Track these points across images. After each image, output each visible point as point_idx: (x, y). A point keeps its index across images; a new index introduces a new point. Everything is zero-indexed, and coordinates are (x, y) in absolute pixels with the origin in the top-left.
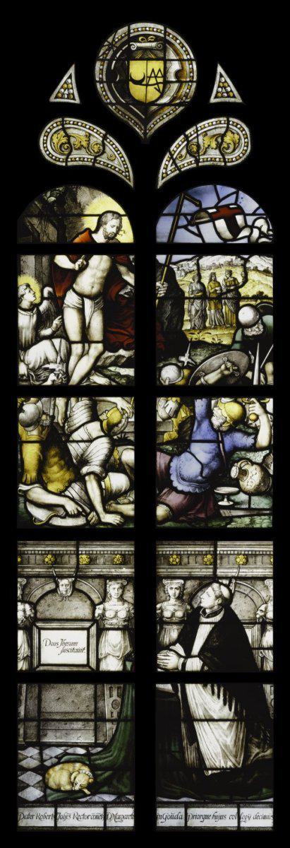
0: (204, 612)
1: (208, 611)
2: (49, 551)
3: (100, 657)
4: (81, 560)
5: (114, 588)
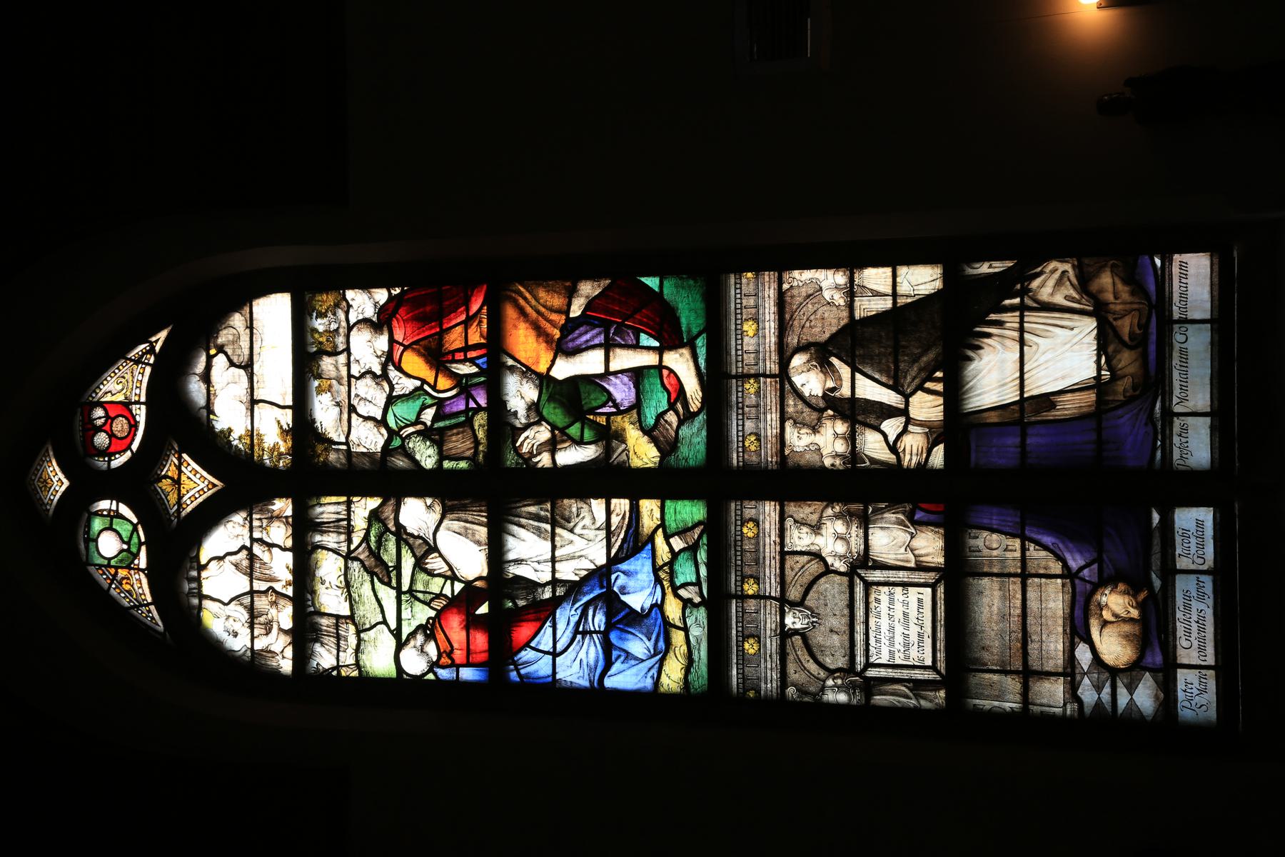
0: (833, 390)
1: (830, 384)
2: (737, 646)
3: (912, 565)
4: (751, 592)
5: (800, 539)
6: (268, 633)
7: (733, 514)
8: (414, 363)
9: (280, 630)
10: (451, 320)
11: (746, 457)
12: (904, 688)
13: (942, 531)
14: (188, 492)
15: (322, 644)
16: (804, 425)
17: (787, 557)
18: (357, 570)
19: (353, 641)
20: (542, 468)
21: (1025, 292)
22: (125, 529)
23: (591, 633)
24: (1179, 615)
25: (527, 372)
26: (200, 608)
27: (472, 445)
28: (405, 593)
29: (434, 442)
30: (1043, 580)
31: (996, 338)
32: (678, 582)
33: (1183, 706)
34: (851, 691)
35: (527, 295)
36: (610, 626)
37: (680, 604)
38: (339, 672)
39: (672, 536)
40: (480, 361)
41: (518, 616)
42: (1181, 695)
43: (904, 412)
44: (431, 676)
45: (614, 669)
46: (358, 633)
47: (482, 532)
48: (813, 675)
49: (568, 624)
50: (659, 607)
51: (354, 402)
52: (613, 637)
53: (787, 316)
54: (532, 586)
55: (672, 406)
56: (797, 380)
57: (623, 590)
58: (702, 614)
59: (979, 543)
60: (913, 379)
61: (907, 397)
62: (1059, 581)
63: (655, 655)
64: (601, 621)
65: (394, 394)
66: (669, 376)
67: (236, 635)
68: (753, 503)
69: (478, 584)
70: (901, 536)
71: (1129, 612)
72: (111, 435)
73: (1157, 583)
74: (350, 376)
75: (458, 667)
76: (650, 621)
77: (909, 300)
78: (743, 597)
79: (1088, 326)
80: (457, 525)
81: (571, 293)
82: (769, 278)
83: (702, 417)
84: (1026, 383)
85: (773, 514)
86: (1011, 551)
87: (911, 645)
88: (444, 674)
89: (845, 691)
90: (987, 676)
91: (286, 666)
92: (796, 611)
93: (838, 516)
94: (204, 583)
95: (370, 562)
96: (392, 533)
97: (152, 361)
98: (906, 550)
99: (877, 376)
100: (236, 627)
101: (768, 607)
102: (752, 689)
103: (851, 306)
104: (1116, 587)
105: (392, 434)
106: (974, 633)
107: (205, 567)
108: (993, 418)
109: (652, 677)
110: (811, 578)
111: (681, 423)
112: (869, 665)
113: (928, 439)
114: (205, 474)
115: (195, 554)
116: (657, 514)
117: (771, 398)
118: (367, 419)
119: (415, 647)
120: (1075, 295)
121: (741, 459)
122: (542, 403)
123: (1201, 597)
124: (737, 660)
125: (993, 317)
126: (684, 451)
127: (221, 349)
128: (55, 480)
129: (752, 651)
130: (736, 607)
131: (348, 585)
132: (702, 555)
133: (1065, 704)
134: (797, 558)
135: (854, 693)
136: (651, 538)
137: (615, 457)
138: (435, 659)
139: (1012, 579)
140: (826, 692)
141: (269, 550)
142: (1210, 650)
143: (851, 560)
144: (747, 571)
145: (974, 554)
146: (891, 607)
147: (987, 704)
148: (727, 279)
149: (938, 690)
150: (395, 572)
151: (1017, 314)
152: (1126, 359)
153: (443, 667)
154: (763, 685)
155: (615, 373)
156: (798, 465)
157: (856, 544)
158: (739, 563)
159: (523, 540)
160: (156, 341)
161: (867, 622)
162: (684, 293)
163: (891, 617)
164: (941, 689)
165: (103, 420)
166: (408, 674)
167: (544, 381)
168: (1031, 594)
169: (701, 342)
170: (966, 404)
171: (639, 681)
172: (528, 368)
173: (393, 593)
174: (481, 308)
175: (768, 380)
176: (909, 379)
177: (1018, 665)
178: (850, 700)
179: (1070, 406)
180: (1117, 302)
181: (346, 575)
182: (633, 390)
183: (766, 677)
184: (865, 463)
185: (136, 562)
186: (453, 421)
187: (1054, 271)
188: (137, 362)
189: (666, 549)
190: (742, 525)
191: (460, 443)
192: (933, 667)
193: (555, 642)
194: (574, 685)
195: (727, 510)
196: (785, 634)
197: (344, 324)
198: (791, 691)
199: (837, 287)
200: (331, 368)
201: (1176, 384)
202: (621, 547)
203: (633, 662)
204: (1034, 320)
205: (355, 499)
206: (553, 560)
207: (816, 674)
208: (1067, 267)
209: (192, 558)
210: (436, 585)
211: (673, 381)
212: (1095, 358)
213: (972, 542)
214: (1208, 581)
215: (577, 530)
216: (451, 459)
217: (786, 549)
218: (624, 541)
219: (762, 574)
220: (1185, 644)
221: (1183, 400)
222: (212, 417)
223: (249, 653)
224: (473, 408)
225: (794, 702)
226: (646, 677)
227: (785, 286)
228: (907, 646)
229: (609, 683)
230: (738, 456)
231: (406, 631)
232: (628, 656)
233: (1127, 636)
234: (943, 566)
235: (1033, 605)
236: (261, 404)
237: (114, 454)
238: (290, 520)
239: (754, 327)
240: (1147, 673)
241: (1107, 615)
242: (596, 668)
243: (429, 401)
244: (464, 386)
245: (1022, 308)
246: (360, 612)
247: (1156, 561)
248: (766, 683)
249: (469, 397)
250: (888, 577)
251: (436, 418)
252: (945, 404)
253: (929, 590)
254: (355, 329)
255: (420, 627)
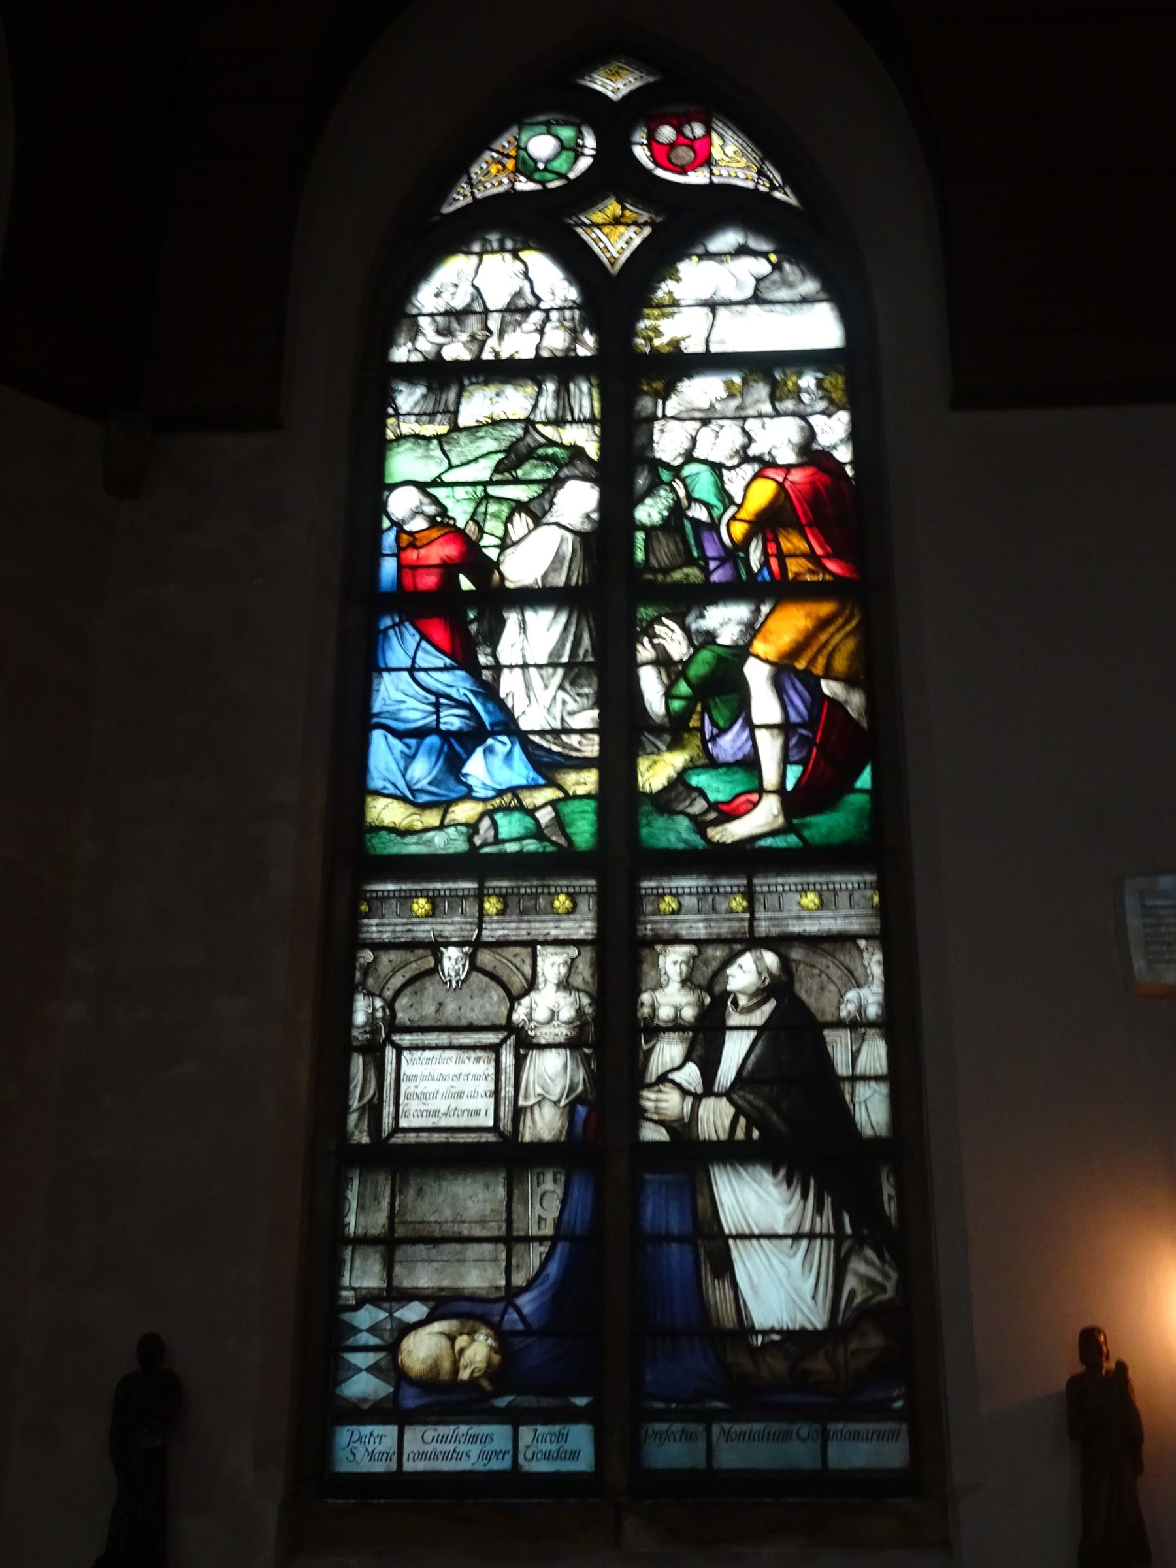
0: (735, 1003)
1: (743, 1001)
2: (421, 891)
3: (521, 1102)
5: (551, 964)
6: (439, 332)
7: (581, 882)
8: (763, 493)
9: (441, 346)
10: (815, 537)
11: (652, 898)
12: (371, 1092)
13: (563, 1138)
14: (606, 235)
15: (424, 397)
16: (692, 968)
17: (530, 950)
18: (513, 434)
19: (429, 430)
20: (635, 650)
21: (859, 1241)
22: (560, 165)
23: (437, 713)
24: (463, 1429)
25: (752, 630)
26: (468, 253)
27: (663, 565)
28: (485, 491)
29: (666, 520)
30: (504, 1264)
31: (801, 1205)
32: (499, 817)
33: (353, 1432)
34: (368, 1029)
35: (848, 628)
36: (446, 736)
37: (472, 821)
38: (391, 416)
39: (555, 810)
40: (766, 572)
41: (458, 626)
42: (366, 1430)
43: (709, 1089)
44: (386, 523)
45: (394, 741)
46: (438, 437)
47: (559, 580)
48: (387, 982)
49: (448, 686)
50: (469, 795)
51: (714, 425)
52: (433, 740)
53: (826, 946)
54: (493, 638)
55: (713, 806)
56: (747, 960)
57: (489, 751)
58: (461, 846)
59: (549, 1185)
60: (749, 1102)
61: (728, 1094)
62: (503, 1283)
63: (412, 791)
64: (452, 724)
65: (724, 471)
66: (751, 802)
67: (437, 295)
68: (595, 908)
69: (496, 575)
70: (556, 1089)
71: (466, 1368)
72: (672, 146)
73: (502, 1402)
74: (745, 419)
75: (397, 555)
76: (452, 783)
77: (848, 1097)
78: (480, 897)
79: (815, 1317)
80: (568, 549)
81: (850, 681)
82: (872, 923)
83: (699, 842)
84: (747, 1242)
85: (582, 931)
86: (539, 1223)
87: (424, 1101)
88: (389, 539)
89: (368, 1021)
90: (388, 1192)
91: (400, 354)
92: (464, 960)
93: (580, 1012)
94: (498, 257)
95: (522, 447)
96: (557, 474)
97: (762, 189)
98: (539, 1095)
99: (752, 1058)
100: (446, 296)
101: (469, 927)
102: (370, 909)
103: (839, 1024)
104: (496, 1352)
105: (676, 471)
106: (438, 1178)
107: (516, 256)
108: (702, 1202)
109: (385, 788)
110: (505, 979)
111: (692, 818)
112: (399, 1050)
113: (676, 1121)
114: (627, 254)
115: (531, 245)
116: (581, 791)
117: (724, 929)
118: (694, 440)
119: (421, 503)
120: (858, 1300)
121: (649, 891)
122: (715, 648)
123: (487, 1456)
124: (405, 891)
125: (828, 1201)
126: (660, 822)
127: (776, 267)
128: (620, 85)
129: (415, 907)
130: (469, 889)
131: (495, 423)
132: (531, 845)
133: (354, 1289)
134: (528, 961)
135: (365, 1032)
136: (552, 783)
137: (651, 737)
138: (407, 528)
139: (504, 1226)
140: (367, 998)
141: (537, 330)
142: (421, 1466)
143: (526, 1028)
144: (513, 901)
145: (535, 1178)
146: (470, 1077)
147: (353, 1195)
148: (871, 872)
149: (370, 1134)
150: (510, 478)
151: (832, 1230)
152: (777, 1365)
153: (397, 539)
154: (374, 921)
155: (753, 737)
156: (643, 962)
157: (545, 1034)
158: (522, 891)
159: (549, 630)
160: (785, 193)
161: (451, 1047)
162: (851, 819)
163: (458, 1077)
164: (370, 1138)
165: (690, 135)
166: (388, 496)
167: (742, 652)
168: (487, 1248)
169: (792, 840)
170: (720, 1171)
171: (380, 772)
172: (757, 631)
173: (485, 477)
174: (830, 572)
175: (746, 924)
176: (751, 1097)
177: (400, 1232)
178: (358, 1027)
179: (719, 1294)
180: (849, 1354)
181: (508, 420)
182: (731, 759)
183: (383, 925)
184: (646, 1043)
185: (522, 179)
186: (692, 541)
187: (886, 1276)
188: (761, 173)
189: (539, 802)
190: (568, 895)
191: (665, 550)
192: (397, 1129)
193: (426, 670)
194: (375, 693)
195: (586, 876)
196: (436, 947)
197: (809, 410)
198: (368, 956)
199: (861, 1008)
200: (756, 396)
201: (746, 1427)
202: (541, 747)
203: (402, 764)
204: (823, 1251)
205: (597, 429)
206: (525, 666)
207: (389, 985)
208: (890, 1292)
209: (527, 243)
210: (494, 527)
211: (743, 808)
212: (777, 1327)
213: (549, 1177)
214: (504, 1464)
215: (561, 695)
216: (647, 542)
217: (539, 947)
218: (549, 751)
219: (508, 918)
220: (428, 1436)
221: (727, 1435)
222: (695, 259)
223: (415, 311)
224: (707, 565)
225: (354, 958)
226: (384, 780)
227: (862, 943)
228: (422, 1096)
229: (377, 736)
230: (652, 888)
231: (440, 493)
232: (410, 758)
233: (437, 1366)
234: (520, 1140)
235: (474, 1250)
236: (711, 315)
237: (650, 149)
238: (572, 354)
239: (812, 906)
240: (391, 1389)
241: (462, 1341)
242: (396, 720)
243: (716, 513)
244: (735, 554)
245: (838, 1236)
246: (463, 438)
247: (529, 1401)
248: (377, 925)
249: (722, 561)
250: (506, 1073)
251: (695, 522)
252: (719, 1142)
253: (490, 1123)
254: (803, 423)
255: (443, 511)
